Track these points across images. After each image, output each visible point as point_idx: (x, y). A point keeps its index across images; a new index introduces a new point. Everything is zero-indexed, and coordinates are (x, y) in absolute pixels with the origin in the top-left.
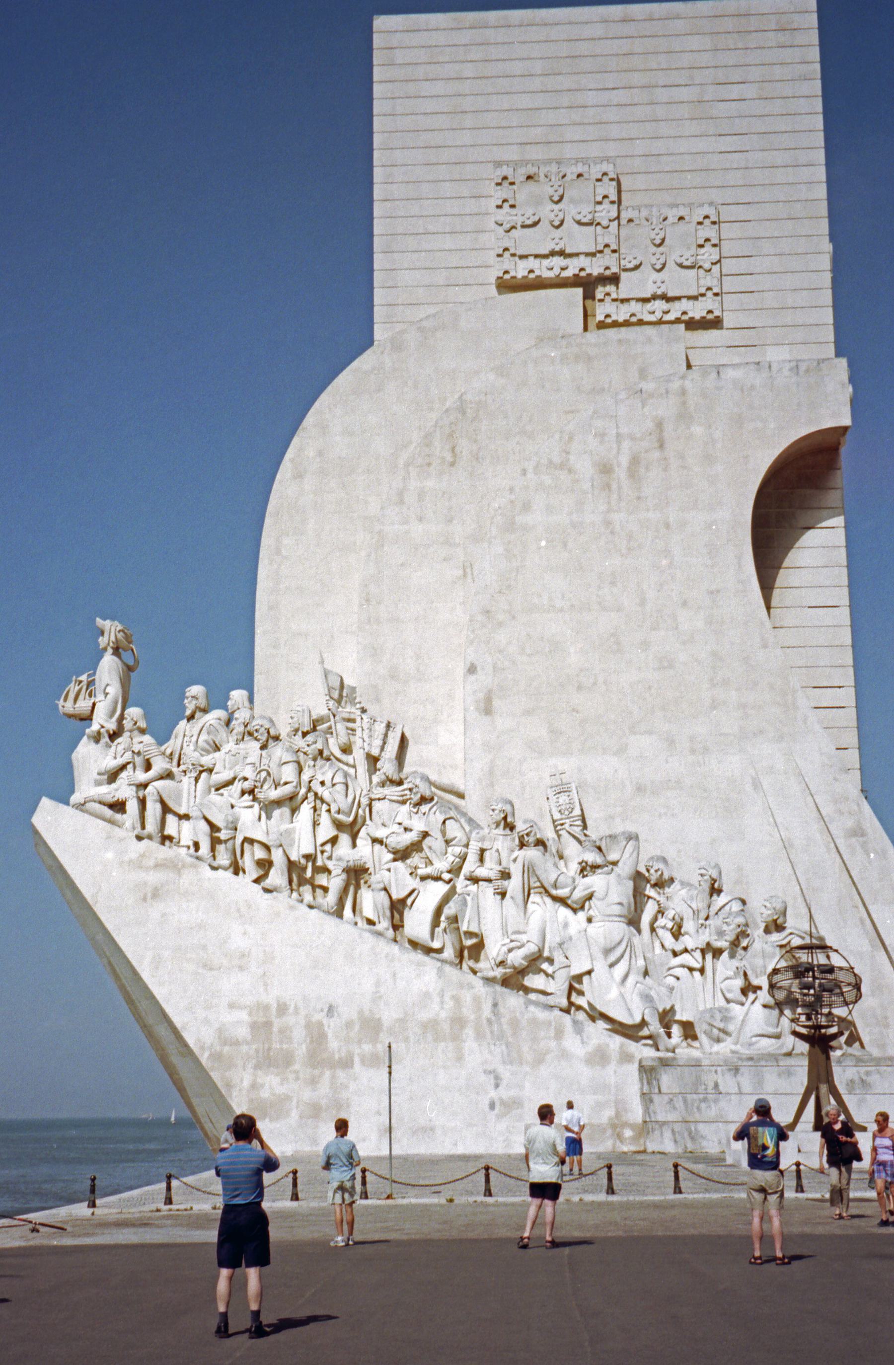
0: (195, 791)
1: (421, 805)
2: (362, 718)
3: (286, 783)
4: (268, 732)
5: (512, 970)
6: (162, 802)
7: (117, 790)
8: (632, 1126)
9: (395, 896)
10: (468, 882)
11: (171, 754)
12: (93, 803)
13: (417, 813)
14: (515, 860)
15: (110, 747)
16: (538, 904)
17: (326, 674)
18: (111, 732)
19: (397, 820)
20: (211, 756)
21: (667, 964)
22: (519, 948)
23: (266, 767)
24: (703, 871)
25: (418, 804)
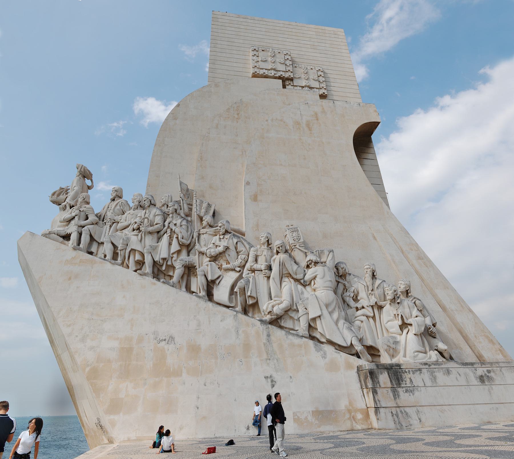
0: (109, 231)
2: (196, 201)
3: (156, 224)
4: (151, 201)
5: (276, 317)
6: (91, 236)
7: (68, 229)
8: (361, 411)
9: (209, 278)
10: (249, 272)
13: (223, 238)
14: (274, 260)
17: (181, 183)
18: (72, 205)
19: (212, 242)
22: (279, 304)
23: (147, 217)
24: (368, 267)
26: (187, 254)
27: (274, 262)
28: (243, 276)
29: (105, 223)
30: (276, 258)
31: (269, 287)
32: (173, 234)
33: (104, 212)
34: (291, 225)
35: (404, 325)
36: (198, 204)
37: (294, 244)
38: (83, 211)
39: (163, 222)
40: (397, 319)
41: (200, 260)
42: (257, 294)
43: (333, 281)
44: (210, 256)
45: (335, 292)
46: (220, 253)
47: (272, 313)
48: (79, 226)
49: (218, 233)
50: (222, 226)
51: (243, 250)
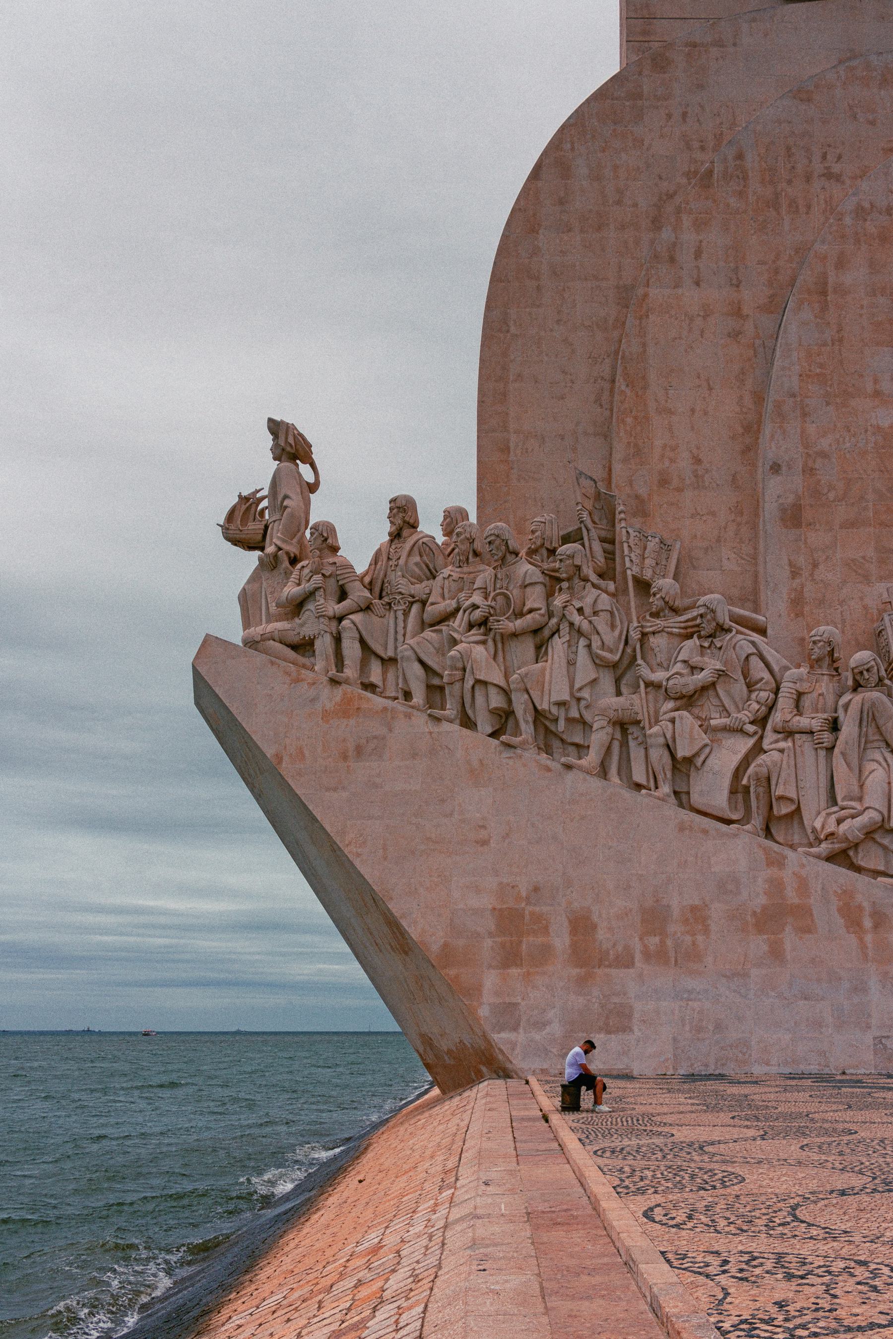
0: (405, 628)
1: (715, 637)
2: (627, 532)
3: (531, 611)
6: (362, 641)
7: (302, 625)
9: (680, 753)
10: (780, 736)
11: (371, 583)
12: (271, 642)
13: (709, 647)
14: (846, 707)
15: (291, 573)
16: (877, 761)
18: (292, 555)
20: (425, 583)
22: (853, 817)
27: (846, 711)
28: (765, 746)
29: (389, 604)
30: (850, 701)
38: (330, 576)
39: (545, 603)
41: (651, 705)
42: (798, 792)
44: (678, 694)
46: (704, 689)
47: (836, 836)
48: (330, 618)
51: (762, 679)
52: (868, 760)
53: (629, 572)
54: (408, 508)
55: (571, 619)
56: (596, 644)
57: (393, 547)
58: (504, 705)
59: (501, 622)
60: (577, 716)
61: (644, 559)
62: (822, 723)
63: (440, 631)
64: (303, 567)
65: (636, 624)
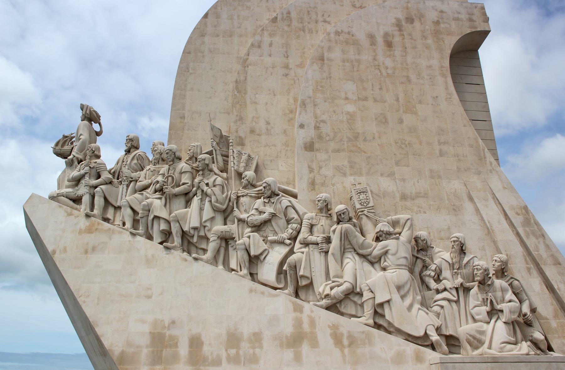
0: (126, 193)
2: (233, 151)
3: (184, 184)
5: (334, 301)
6: (106, 199)
7: (78, 190)
9: (252, 253)
11: (114, 172)
12: (62, 197)
13: (268, 202)
14: (334, 231)
16: (350, 258)
17: (213, 128)
18: (79, 159)
20: (138, 172)
21: (433, 299)
22: (338, 286)
24: (455, 239)
25: (269, 197)
26: (223, 222)
28: (295, 251)
29: (121, 181)
30: (336, 228)
31: (327, 264)
32: (205, 196)
33: (118, 167)
34: (358, 184)
35: (493, 313)
36: (235, 156)
37: (360, 210)
38: (93, 168)
40: (486, 304)
41: (240, 230)
42: (311, 274)
43: (409, 258)
44: (253, 225)
45: (411, 271)
47: (329, 296)
48: (90, 187)
49: (261, 195)
50: (266, 187)
51: (294, 218)
52: (346, 258)
53: (233, 168)
54: (134, 139)
55: (203, 188)
56: (213, 199)
57: (126, 156)
58: (168, 229)
59: (168, 189)
60: (203, 234)
61: (240, 163)
62: (322, 239)
63: (142, 194)
64: (82, 164)
65: (234, 192)
